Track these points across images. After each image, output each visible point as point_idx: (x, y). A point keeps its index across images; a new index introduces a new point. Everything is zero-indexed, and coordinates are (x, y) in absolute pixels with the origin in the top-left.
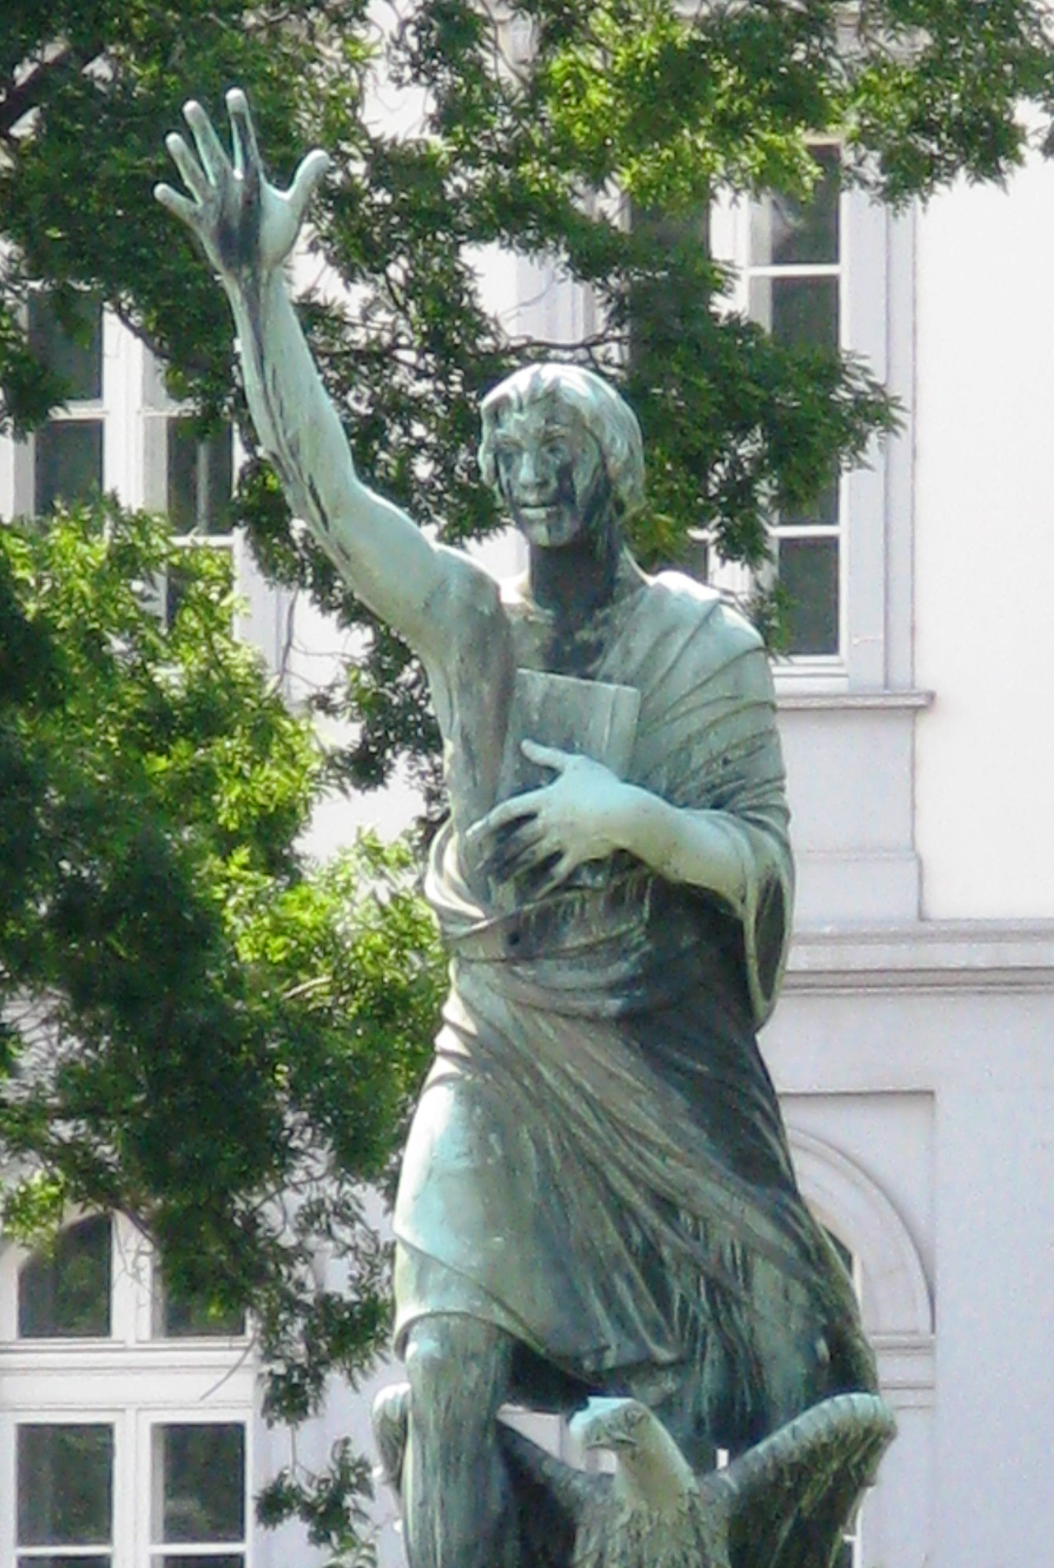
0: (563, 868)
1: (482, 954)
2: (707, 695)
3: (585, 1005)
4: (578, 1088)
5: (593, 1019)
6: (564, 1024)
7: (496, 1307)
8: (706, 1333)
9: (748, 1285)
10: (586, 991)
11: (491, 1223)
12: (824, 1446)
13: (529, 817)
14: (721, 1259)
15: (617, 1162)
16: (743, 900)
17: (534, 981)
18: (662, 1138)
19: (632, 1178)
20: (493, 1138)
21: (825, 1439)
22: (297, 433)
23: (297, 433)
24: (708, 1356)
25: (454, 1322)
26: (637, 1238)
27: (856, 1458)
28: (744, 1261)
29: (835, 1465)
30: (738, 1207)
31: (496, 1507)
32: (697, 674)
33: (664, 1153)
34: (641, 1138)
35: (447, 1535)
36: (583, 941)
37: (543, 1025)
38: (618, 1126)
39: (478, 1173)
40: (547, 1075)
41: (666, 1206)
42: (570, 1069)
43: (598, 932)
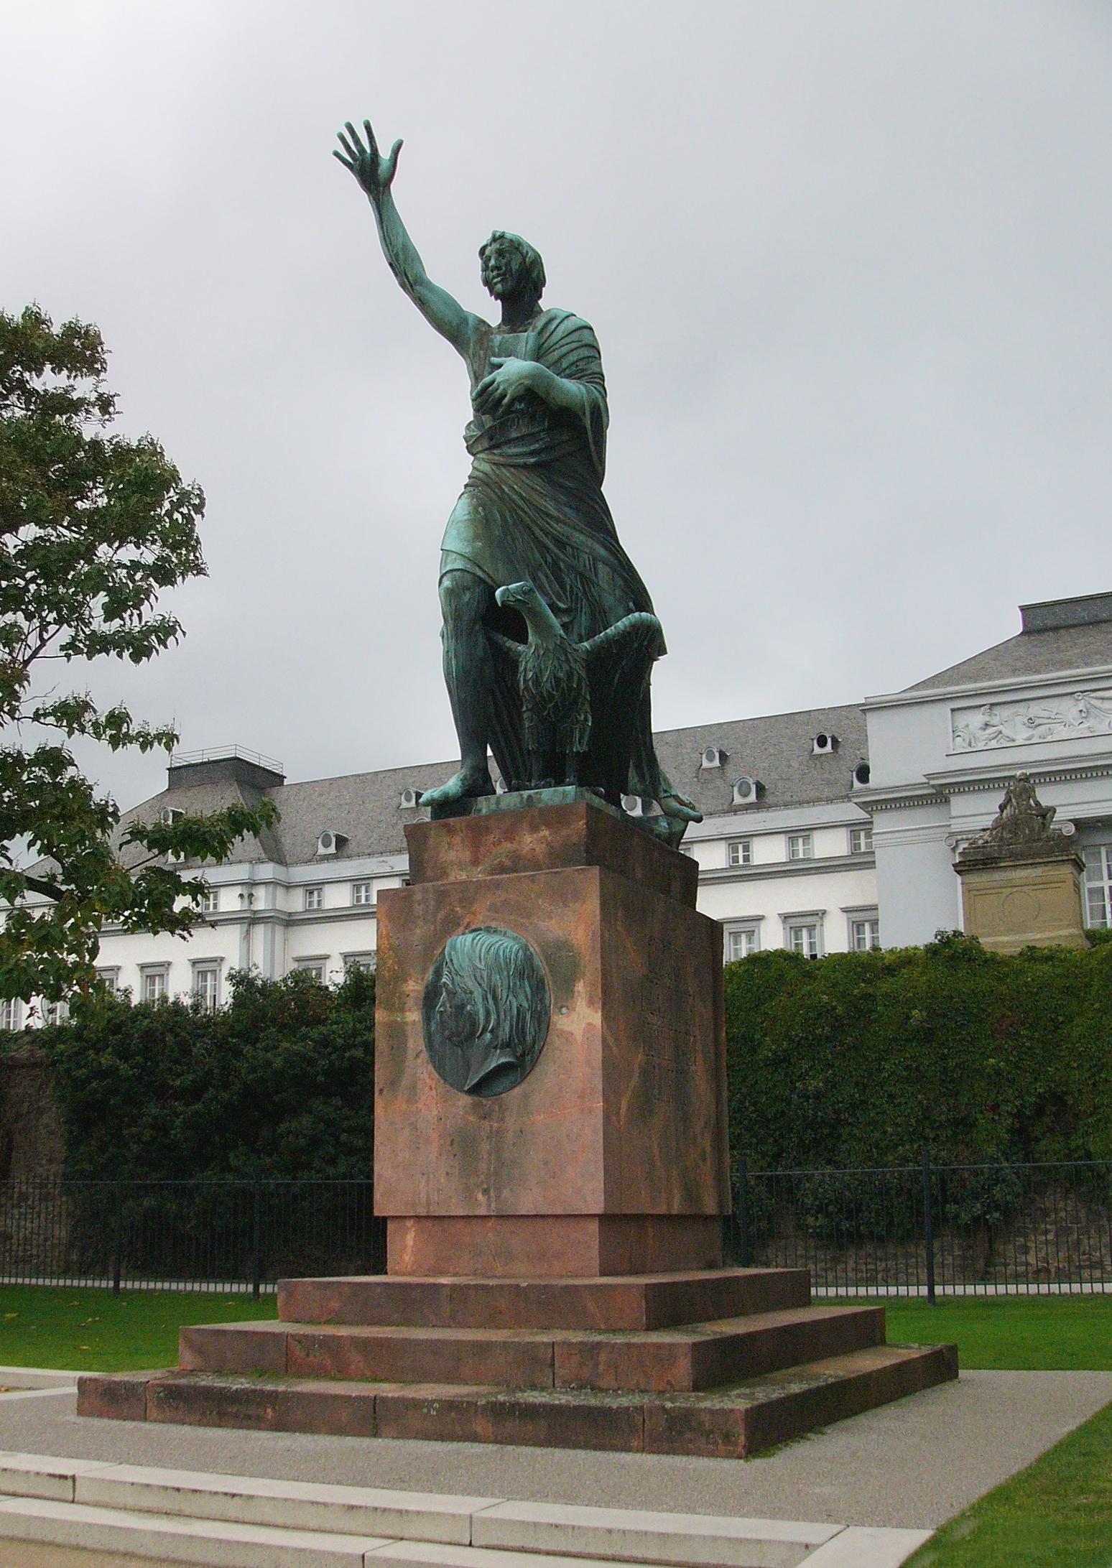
0: (506, 400)
1: (480, 449)
2: (568, 340)
3: (521, 461)
4: (520, 495)
5: (525, 467)
6: (512, 469)
7: (477, 569)
8: (582, 601)
9: (596, 575)
10: (522, 455)
11: (476, 537)
12: (629, 633)
13: (493, 382)
14: (585, 566)
15: (537, 525)
16: (584, 413)
17: (500, 455)
18: (555, 513)
19: (546, 534)
20: (480, 509)
21: (628, 630)
22: (397, 252)
23: (397, 252)
24: (584, 610)
25: (458, 574)
26: (550, 560)
27: (645, 643)
28: (594, 564)
29: (636, 645)
30: (590, 542)
31: (480, 652)
32: (563, 332)
33: (558, 521)
34: (548, 515)
35: (457, 665)
36: (519, 435)
37: (505, 471)
38: (537, 509)
39: (472, 522)
40: (506, 490)
41: (560, 544)
42: (515, 487)
43: (524, 431)
